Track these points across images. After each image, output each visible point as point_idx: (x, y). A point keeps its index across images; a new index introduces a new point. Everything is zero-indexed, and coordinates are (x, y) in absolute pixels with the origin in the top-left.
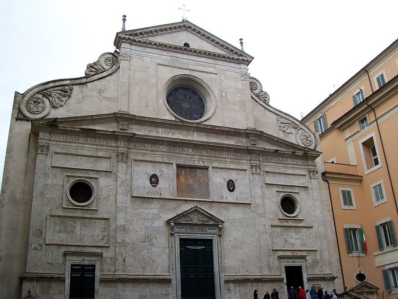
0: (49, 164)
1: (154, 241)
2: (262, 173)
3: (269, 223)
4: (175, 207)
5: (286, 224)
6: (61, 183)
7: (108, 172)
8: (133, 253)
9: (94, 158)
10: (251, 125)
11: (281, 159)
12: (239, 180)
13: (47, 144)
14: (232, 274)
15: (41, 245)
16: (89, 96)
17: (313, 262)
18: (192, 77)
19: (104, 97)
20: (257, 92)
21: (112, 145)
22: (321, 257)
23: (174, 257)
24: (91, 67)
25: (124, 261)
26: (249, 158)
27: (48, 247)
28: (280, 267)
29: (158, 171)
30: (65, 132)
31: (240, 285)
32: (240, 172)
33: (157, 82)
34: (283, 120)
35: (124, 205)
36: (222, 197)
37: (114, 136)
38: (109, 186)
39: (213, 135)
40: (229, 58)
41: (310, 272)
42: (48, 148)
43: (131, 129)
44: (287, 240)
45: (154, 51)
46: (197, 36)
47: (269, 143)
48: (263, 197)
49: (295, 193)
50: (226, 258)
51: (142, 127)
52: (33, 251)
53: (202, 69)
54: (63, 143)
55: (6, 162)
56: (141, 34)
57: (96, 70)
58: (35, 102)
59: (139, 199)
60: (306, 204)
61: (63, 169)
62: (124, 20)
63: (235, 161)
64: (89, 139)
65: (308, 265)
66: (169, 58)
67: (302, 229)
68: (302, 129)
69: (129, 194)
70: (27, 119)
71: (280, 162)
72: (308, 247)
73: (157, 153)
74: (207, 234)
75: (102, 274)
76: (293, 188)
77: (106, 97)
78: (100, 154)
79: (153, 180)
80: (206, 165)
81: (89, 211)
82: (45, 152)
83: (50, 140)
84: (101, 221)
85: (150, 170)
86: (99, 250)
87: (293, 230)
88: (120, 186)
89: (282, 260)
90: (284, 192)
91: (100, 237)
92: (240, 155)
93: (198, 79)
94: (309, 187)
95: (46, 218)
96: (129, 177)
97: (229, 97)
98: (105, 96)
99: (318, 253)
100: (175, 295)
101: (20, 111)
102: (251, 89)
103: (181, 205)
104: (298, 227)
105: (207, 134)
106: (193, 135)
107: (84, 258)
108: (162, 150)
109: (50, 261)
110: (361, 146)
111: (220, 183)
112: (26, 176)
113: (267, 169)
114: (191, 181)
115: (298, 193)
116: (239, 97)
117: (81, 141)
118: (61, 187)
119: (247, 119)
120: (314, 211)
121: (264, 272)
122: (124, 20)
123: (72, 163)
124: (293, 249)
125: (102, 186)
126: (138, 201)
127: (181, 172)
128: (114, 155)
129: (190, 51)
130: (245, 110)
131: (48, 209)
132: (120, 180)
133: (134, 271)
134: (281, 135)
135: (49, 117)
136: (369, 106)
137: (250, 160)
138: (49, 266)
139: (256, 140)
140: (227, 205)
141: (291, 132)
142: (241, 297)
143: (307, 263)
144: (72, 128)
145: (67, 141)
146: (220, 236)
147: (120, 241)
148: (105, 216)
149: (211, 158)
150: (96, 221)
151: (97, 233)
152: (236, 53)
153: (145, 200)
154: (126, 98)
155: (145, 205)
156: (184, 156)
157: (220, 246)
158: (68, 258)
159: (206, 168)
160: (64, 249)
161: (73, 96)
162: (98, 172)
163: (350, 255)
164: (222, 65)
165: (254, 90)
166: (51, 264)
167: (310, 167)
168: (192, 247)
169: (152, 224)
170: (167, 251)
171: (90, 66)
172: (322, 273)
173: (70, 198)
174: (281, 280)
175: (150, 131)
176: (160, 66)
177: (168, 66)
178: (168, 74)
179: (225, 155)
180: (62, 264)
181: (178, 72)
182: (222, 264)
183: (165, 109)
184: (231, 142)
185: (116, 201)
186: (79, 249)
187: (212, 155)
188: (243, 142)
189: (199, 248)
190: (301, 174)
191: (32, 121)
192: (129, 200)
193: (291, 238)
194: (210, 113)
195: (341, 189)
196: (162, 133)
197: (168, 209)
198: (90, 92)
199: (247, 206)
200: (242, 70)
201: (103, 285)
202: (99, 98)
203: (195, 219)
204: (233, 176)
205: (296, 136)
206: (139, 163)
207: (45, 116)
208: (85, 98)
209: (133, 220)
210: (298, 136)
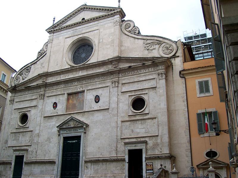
1: (51, 140)
2: (120, 85)
3: (120, 120)
6: (17, 116)
8: (41, 148)
9: (30, 101)
10: (116, 54)
11: (136, 71)
12: (103, 94)
14: (90, 157)
17: (153, 145)
18: (83, 38)
26: (112, 77)
28: (124, 151)
29: (58, 100)
30: (20, 91)
31: (95, 164)
32: (105, 88)
34: (149, 42)
37: (38, 87)
39: (90, 69)
40: (106, 16)
41: (150, 153)
45: (65, 31)
47: (128, 62)
49: (144, 94)
50: (88, 147)
53: (90, 30)
58: (17, 79)
60: (153, 101)
66: (72, 31)
67: (147, 121)
68: (164, 42)
69: (43, 116)
71: (135, 74)
72: (151, 134)
73: (59, 90)
74: (77, 133)
76: (143, 90)
78: (33, 98)
79: (54, 105)
82: (12, 103)
84: (30, 132)
85: (54, 100)
87: (140, 122)
88: (39, 113)
91: (29, 140)
93: (87, 38)
97: (104, 41)
99: (159, 137)
100: (57, 171)
104: (144, 119)
105: (87, 70)
107: (20, 152)
111: (91, 99)
113: (124, 82)
114: (75, 101)
115: (147, 93)
116: (111, 38)
117: (27, 93)
120: (160, 104)
121: (112, 155)
125: (32, 114)
126: (47, 119)
127: (70, 98)
129: (86, 21)
131: (11, 130)
133: (40, 158)
138: (8, 157)
139: (117, 64)
140: (92, 112)
141: (154, 48)
142: (94, 172)
143: (148, 146)
144: (21, 88)
146: (85, 133)
147: (36, 142)
148: (32, 130)
149: (87, 84)
150: (28, 133)
151: (27, 139)
152: (111, 10)
153: (50, 118)
155: (49, 121)
156: (72, 87)
159: (83, 92)
161: (31, 71)
163: (202, 136)
165: (128, 28)
166: (9, 156)
168: (70, 142)
170: (57, 145)
172: (161, 153)
175: (57, 78)
176: (67, 39)
177: (70, 37)
178: (70, 41)
179: (96, 80)
181: (76, 38)
188: (110, 67)
189: (74, 141)
193: (136, 129)
195: (197, 81)
196: (63, 77)
197: (60, 121)
201: (26, 165)
203: (72, 124)
204: (99, 92)
205: (158, 50)
206: (49, 98)
210: (161, 49)
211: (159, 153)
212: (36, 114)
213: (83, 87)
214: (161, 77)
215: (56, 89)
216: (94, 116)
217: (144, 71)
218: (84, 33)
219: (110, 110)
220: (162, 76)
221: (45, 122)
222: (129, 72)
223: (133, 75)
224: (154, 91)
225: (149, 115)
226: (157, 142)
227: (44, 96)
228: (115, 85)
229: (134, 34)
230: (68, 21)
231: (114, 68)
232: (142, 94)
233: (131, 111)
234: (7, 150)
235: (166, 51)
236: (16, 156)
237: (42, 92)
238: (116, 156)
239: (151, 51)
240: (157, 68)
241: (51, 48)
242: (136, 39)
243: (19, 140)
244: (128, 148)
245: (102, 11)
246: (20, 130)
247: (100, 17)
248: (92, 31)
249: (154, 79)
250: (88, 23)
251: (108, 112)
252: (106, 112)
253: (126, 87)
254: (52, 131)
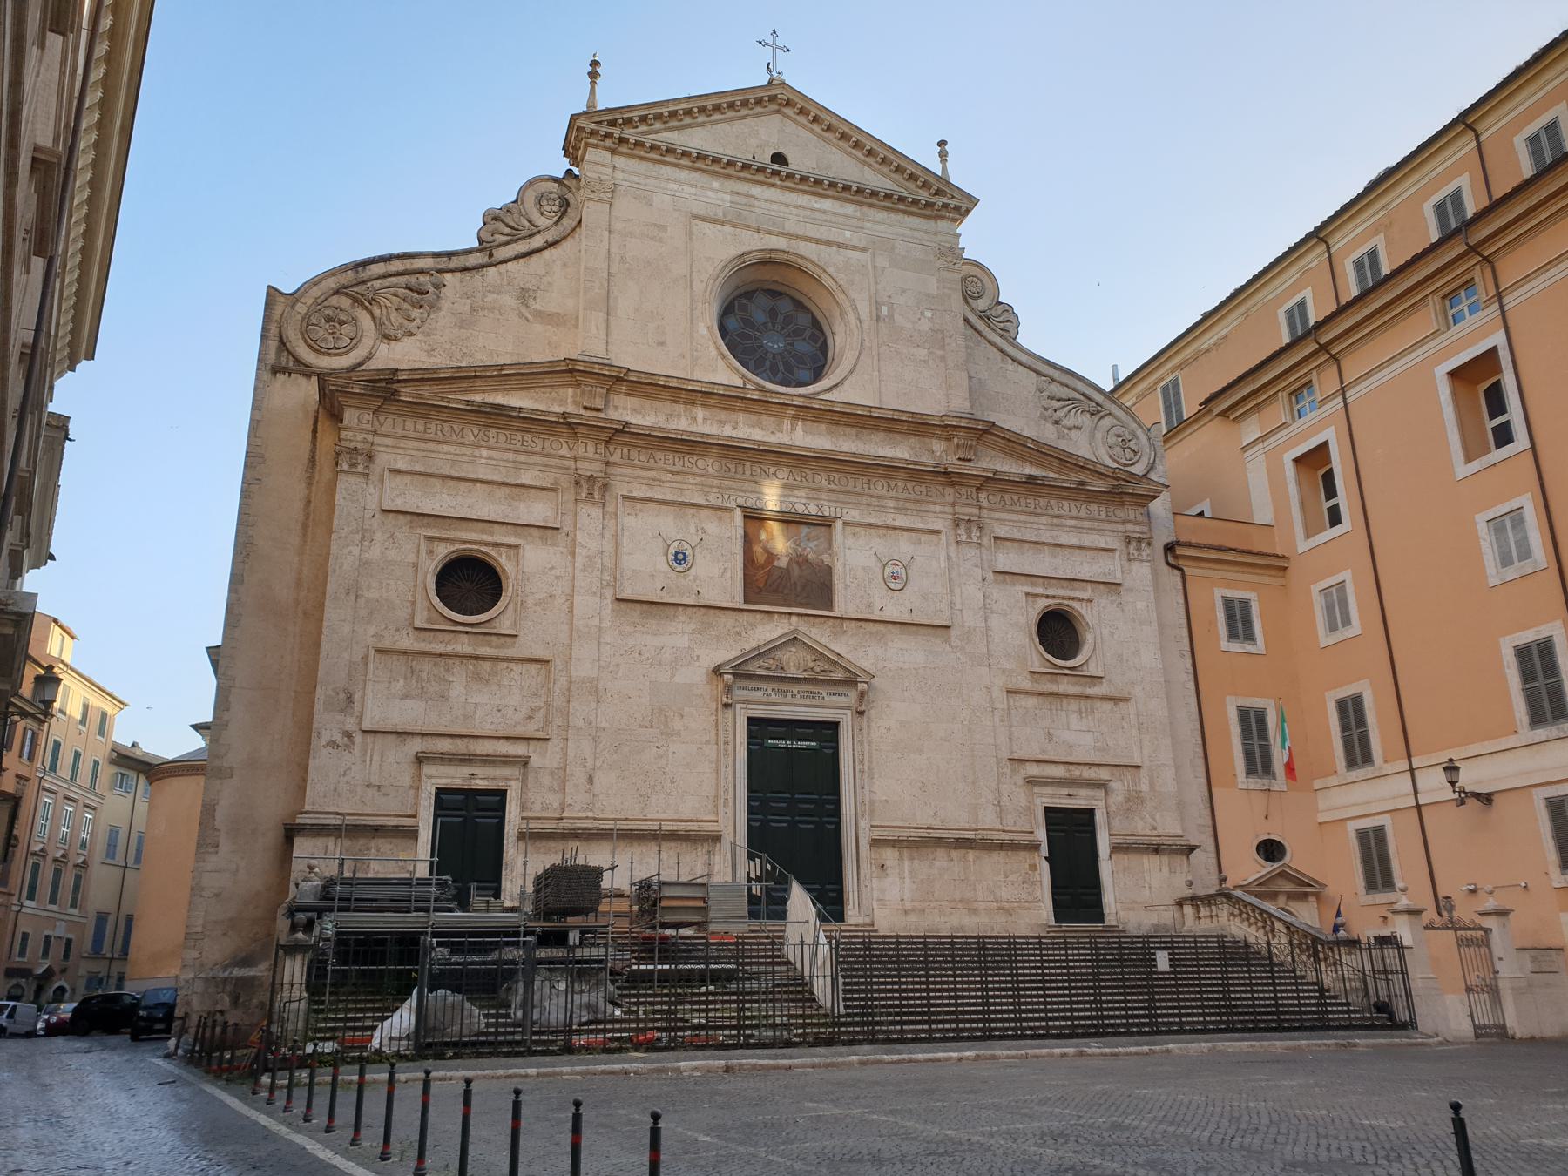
0: (373, 504)
1: (677, 724)
2: (985, 541)
4: (737, 629)
5: (1053, 688)
6: (411, 558)
9: (507, 490)
10: (959, 404)
11: (1043, 502)
13: (367, 446)
15: (348, 735)
16: (494, 308)
17: (1128, 800)
19: (535, 310)
20: (982, 304)
21: (562, 452)
22: (1152, 785)
23: (730, 770)
24: (496, 219)
25: (591, 780)
26: (950, 499)
27: (370, 738)
28: (1029, 810)
29: (692, 529)
30: (419, 409)
32: (924, 537)
33: (692, 272)
34: (1055, 389)
35: (596, 621)
36: (870, 606)
37: (567, 426)
38: (553, 568)
39: (848, 430)
41: (1118, 825)
42: (370, 458)
43: (616, 408)
44: (1051, 731)
46: (812, 131)
47: (1011, 455)
48: (987, 610)
49: (1081, 600)
51: (647, 403)
52: (324, 752)
54: (415, 444)
55: (245, 495)
56: (643, 119)
57: (512, 228)
58: (329, 320)
59: (638, 605)
60: (1112, 634)
61: (415, 518)
62: (593, 75)
63: (908, 505)
64: (492, 433)
65: (1113, 808)
67: (1098, 704)
69: (609, 594)
70: (307, 371)
71: (1039, 511)
74: (819, 707)
75: (525, 814)
76: (1077, 584)
77: (540, 311)
78: (526, 478)
81: (493, 638)
82: (360, 468)
83: (375, 433)
86: (518, 749)
87: (1074, 705)
88: (583, 571)
89: (1036, 789)
90: (1047, 596)
91: (524, 712)
92: (923, 488)
94: (1127, 584)
95: (365, 659)
96: (608, 547)
98: (538, 307)
99: (1143, 772)
101: (282, 343)
102: (966, 297)
103: (753, 626)
106: (793, 429)
108: (703, 472)
109: (375, 780)
110: (1290, 470)
111: (864, 568)
112: (304, 535)
113: (1001, 531)
117: (469, 437)
118: (411, 570)
119: (949, 387)
122: (593, 75)
123: (441, 501)
124: (1069, 759)
128: (565, 481)
129: (790, 176)
130: (943, 359)
131: (372, 630)
132: (584, 552)
134: (1048, 435)
135: (373, 365)
136: (1323, 348)
137: (953, 505)
140: (881, 627)
141: (1078, 423)
143: (1111, 800)
144: (442, 399)
145: (427, 436)
147: (581, 723)
150: (512, 665)
154: (602, 315)
157: (861, 742)
158: (428, 769)
159: (826, 523)
160: (416, 745)
161: (445, 304)
162: (519, 529)
164: (881, 223)
165: (971, 297)
167: (1130, 527)
168: (782, 744)
169: (673, 675)
170: (711, 751)
171: (492, 218)
172: (1155, 833)
173: (436, 601)
174: (1034, 847)
179: (880, 487)
180: (412, 787)
181: (753, 243)
182: (866, 791)
183: (714, 352)
184: (899, 450)
185: (571, 612)
186: (461, 747)
187: (844, 489)
189: (803, 744)
190: (1103, 546)
191: (322, 377)
192: (609, 611)
194: (841, 366)
195: (1219, 593)
198: (495, 296)
199: (939, 631)
200: (940, 237)
202: (521, 315)
203: (794, 662)
204: (904, 547)
206: (639, 505)
207: (361, 364)
208: (481, 313)
209: (618, 665)
211: (1149, 833)
212: (556, 572)
214: (1136, 553)
215: (678, 473)
216: (886, 644)
217: (1074, 513)
218: (799, 238)
219: (953, 632)
220: (1139, 549)
221: (628, 629)
222: (1016, 497)
223: (1036, 514)
224: (1113, 598)
225: (1101, 683)
226: (1138, 789)
227: (605, 487)
229: (1001, 336)
230: (697, 125)
231: (960, 459)
232: (1073, 599)
233: (1036, 657)
234: (357, 749)
235: (1118, 450)
236: (440, 792)
237: (587, 465)
238: (1001, 827)
239: (1066, 431)
240: (1120, 513)
241: (610, 231)
242: (1010, 361)
243: (444, 697)
244: (1044, 800)
245: (877, 166)
246: (449, 642)
247: (874, 194)
248: (838, 245)
249: (1113, 550)
250: (813, 194)
251: (947, 640)
252: (938, 641)
253: (1011, 555)
254: (679, 679)
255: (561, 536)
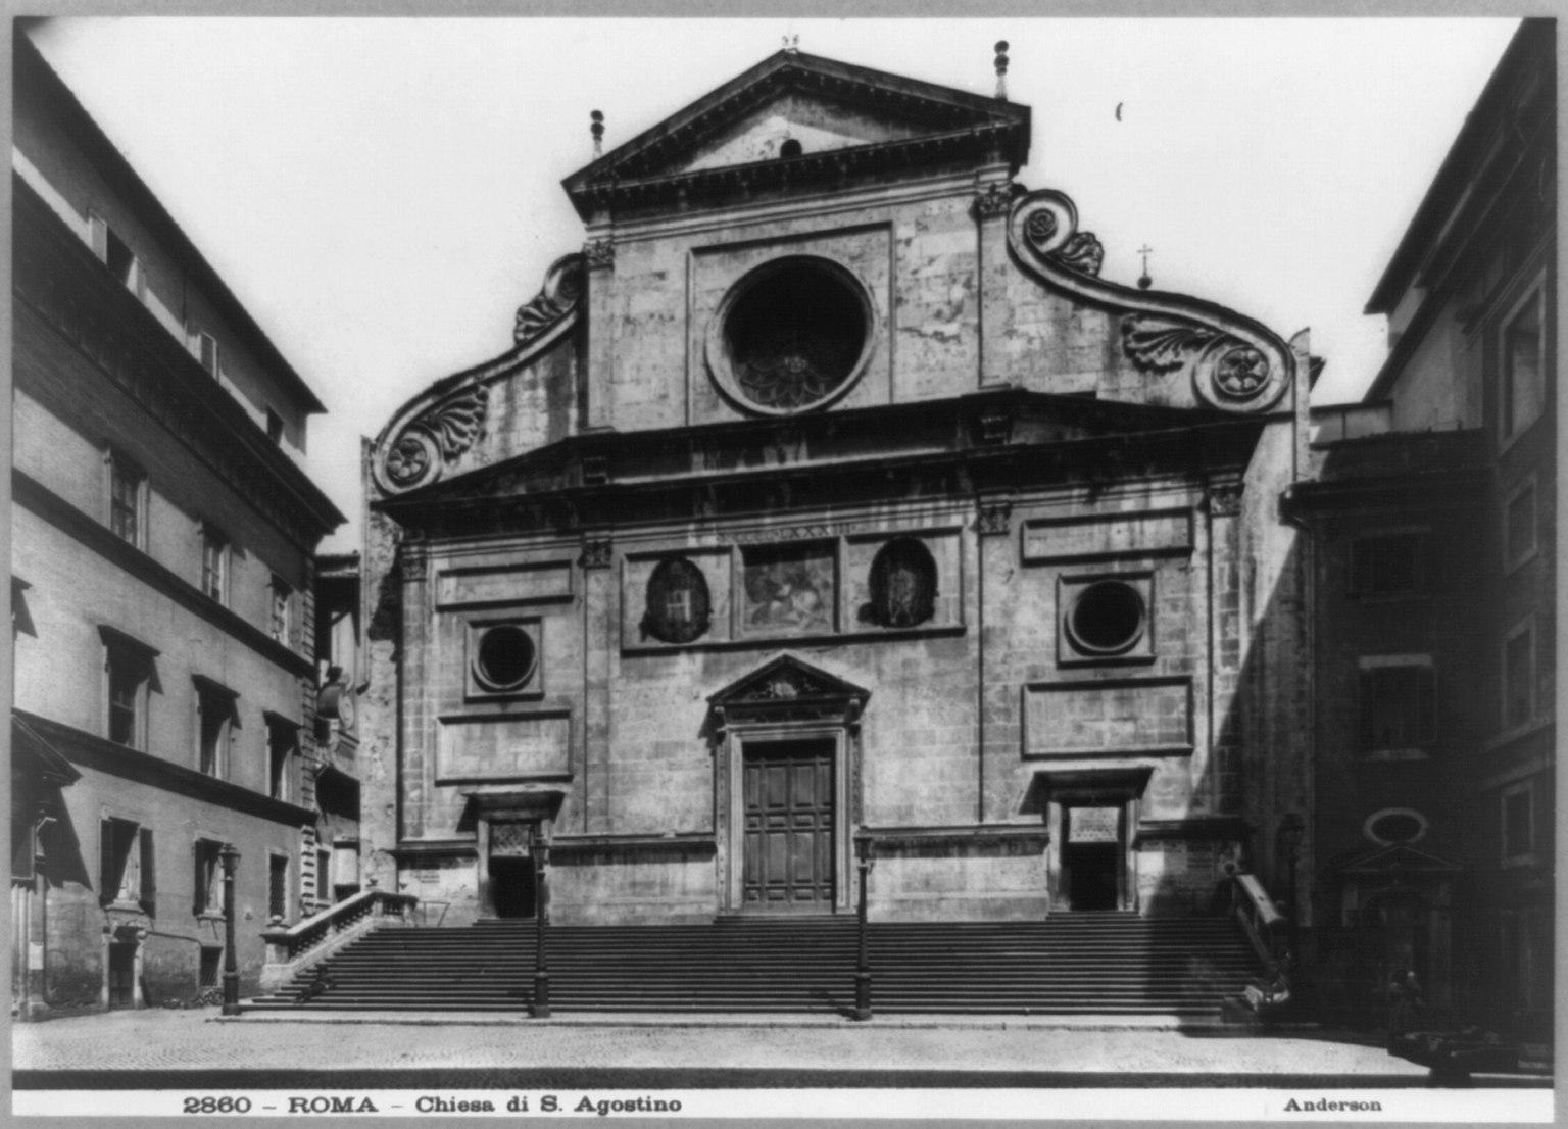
7: (563, 600)
80: (830, 532)
203: (784, 689)
213: (828, 522)
228: (994, 526)
255: (575, 602)
